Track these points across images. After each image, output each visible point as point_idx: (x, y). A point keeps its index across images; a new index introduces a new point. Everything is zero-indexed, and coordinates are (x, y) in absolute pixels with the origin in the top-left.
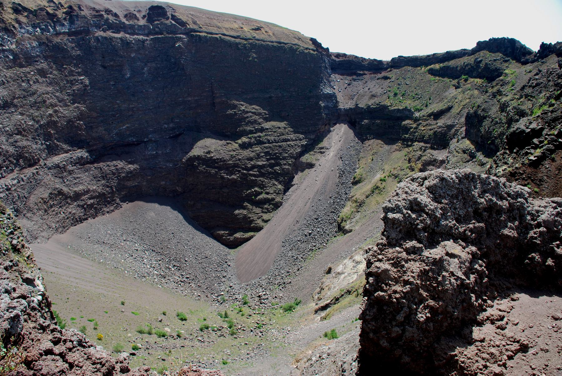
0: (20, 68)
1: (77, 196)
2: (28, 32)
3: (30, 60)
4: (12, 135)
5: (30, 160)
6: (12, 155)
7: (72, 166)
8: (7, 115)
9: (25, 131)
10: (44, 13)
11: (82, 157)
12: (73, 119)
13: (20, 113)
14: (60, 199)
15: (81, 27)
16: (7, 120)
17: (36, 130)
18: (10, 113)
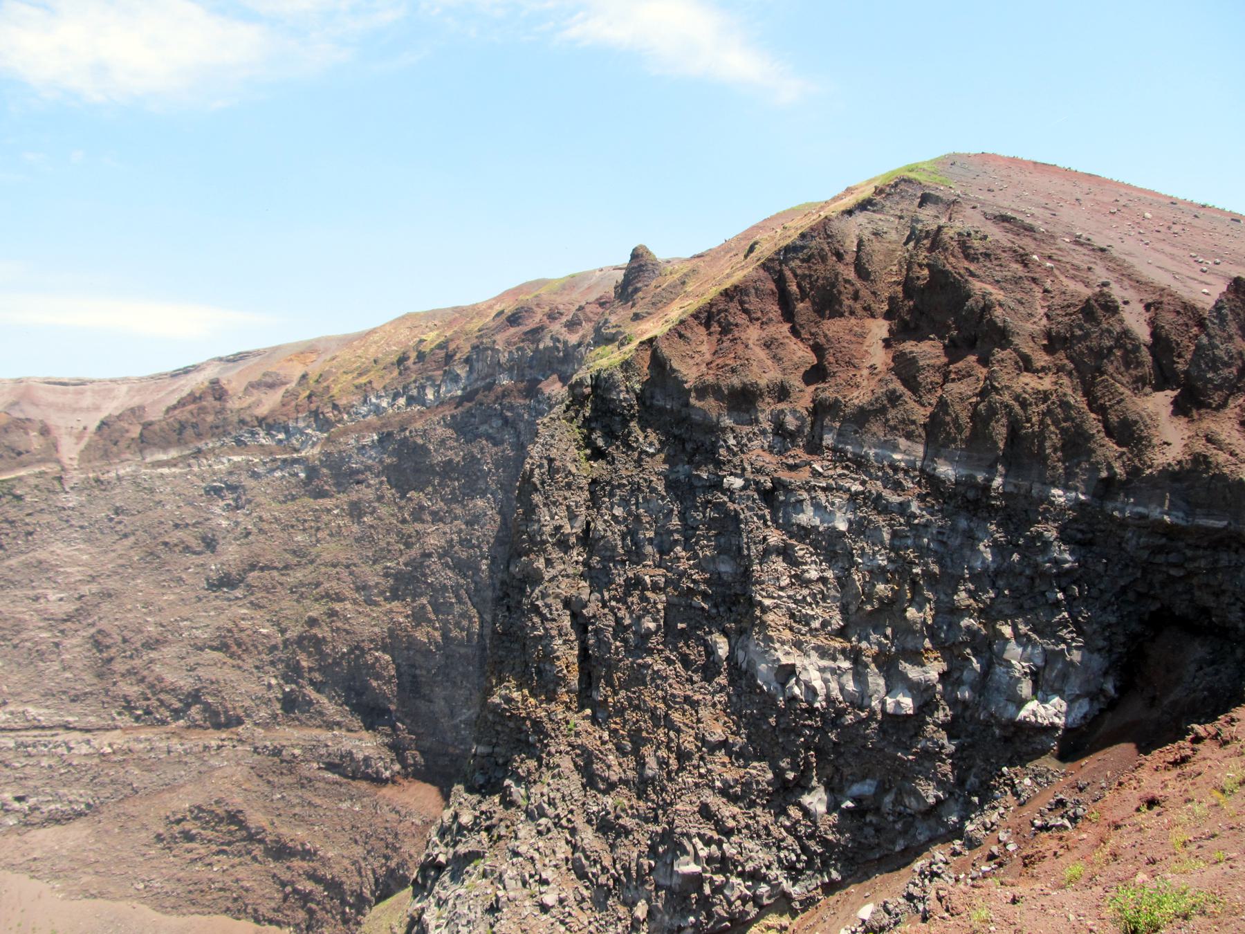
0: (315, 498)
1: (281, 851)
2: (378, 410)
3: (344, 475)
4: (201, 649)
5: (217, 714)
6: (173, 691)
7: (319, 768)
8: (218, 603)
9: (239, 645)
10: (442, 353)
11: (350, 753)
12: (366, 645)
13: (251, 603)
14: (230, 832)
15: (484, 379)
16: (212, 613)
17: (274, 648)
18: (229, 600)
